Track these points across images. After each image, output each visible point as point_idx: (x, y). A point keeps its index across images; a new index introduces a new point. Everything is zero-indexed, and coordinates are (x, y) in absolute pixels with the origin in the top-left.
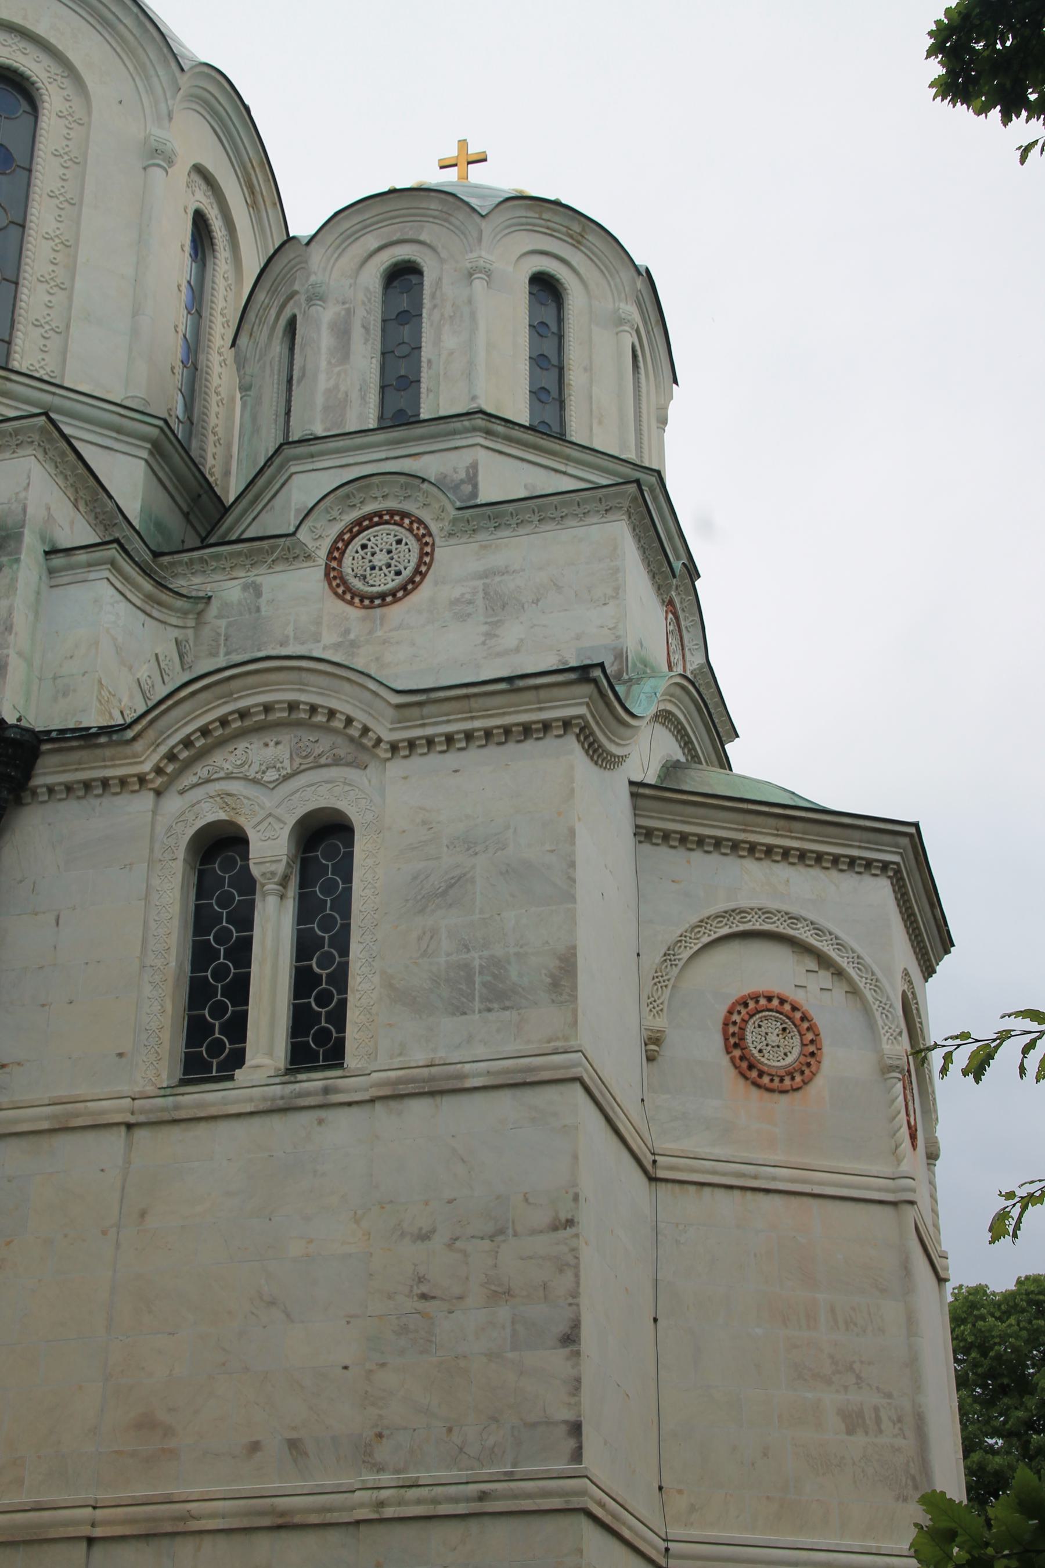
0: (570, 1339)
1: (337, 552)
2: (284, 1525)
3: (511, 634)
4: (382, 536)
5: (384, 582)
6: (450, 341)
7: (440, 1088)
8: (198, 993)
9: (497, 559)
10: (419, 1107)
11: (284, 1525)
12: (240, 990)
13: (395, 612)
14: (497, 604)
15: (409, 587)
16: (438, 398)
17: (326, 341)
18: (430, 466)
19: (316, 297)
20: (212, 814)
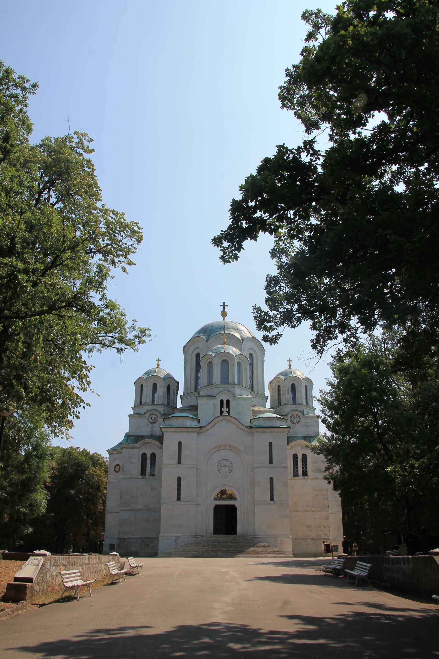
0: (328, 499)
1: (291, 418)
2: (307, 511)
3: (309, 429)
4: (295, 416)
5: (295, 422)
6: (299, 394)
7: (317, 478)
8: (294, 468)
9: (307, 421)
10: (315, 480)
11: (307, 511)
12: (297, 468)
13: (297, 425)
14: (307, 426)
15: (298, 423)
16: (298, 401)
17: (286, 392)
18: (299, 409)
19: (285, 386)
20: (295, 453)
